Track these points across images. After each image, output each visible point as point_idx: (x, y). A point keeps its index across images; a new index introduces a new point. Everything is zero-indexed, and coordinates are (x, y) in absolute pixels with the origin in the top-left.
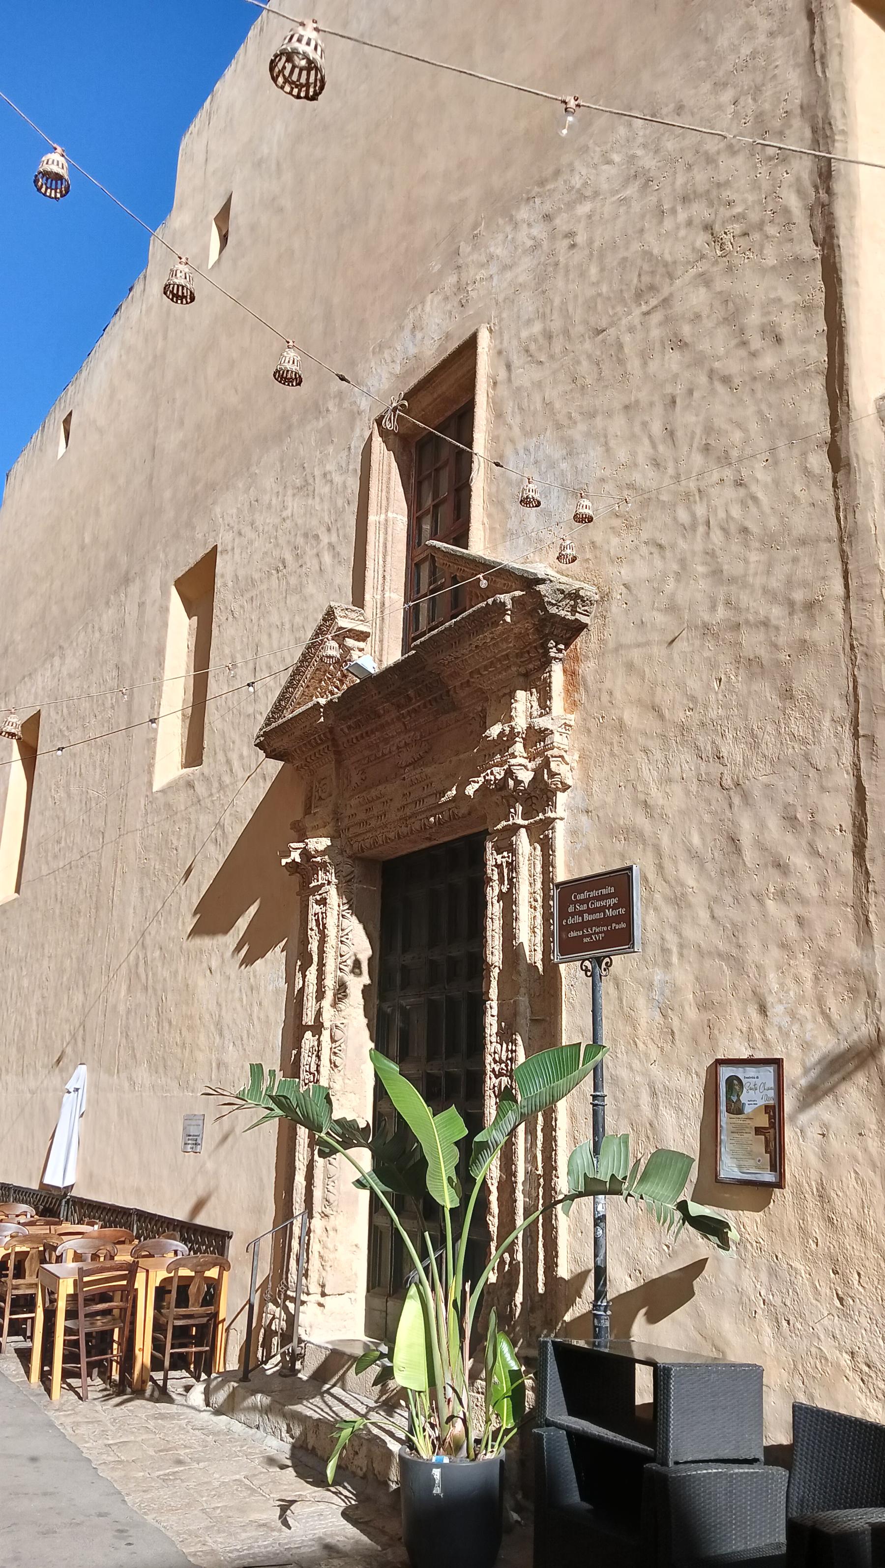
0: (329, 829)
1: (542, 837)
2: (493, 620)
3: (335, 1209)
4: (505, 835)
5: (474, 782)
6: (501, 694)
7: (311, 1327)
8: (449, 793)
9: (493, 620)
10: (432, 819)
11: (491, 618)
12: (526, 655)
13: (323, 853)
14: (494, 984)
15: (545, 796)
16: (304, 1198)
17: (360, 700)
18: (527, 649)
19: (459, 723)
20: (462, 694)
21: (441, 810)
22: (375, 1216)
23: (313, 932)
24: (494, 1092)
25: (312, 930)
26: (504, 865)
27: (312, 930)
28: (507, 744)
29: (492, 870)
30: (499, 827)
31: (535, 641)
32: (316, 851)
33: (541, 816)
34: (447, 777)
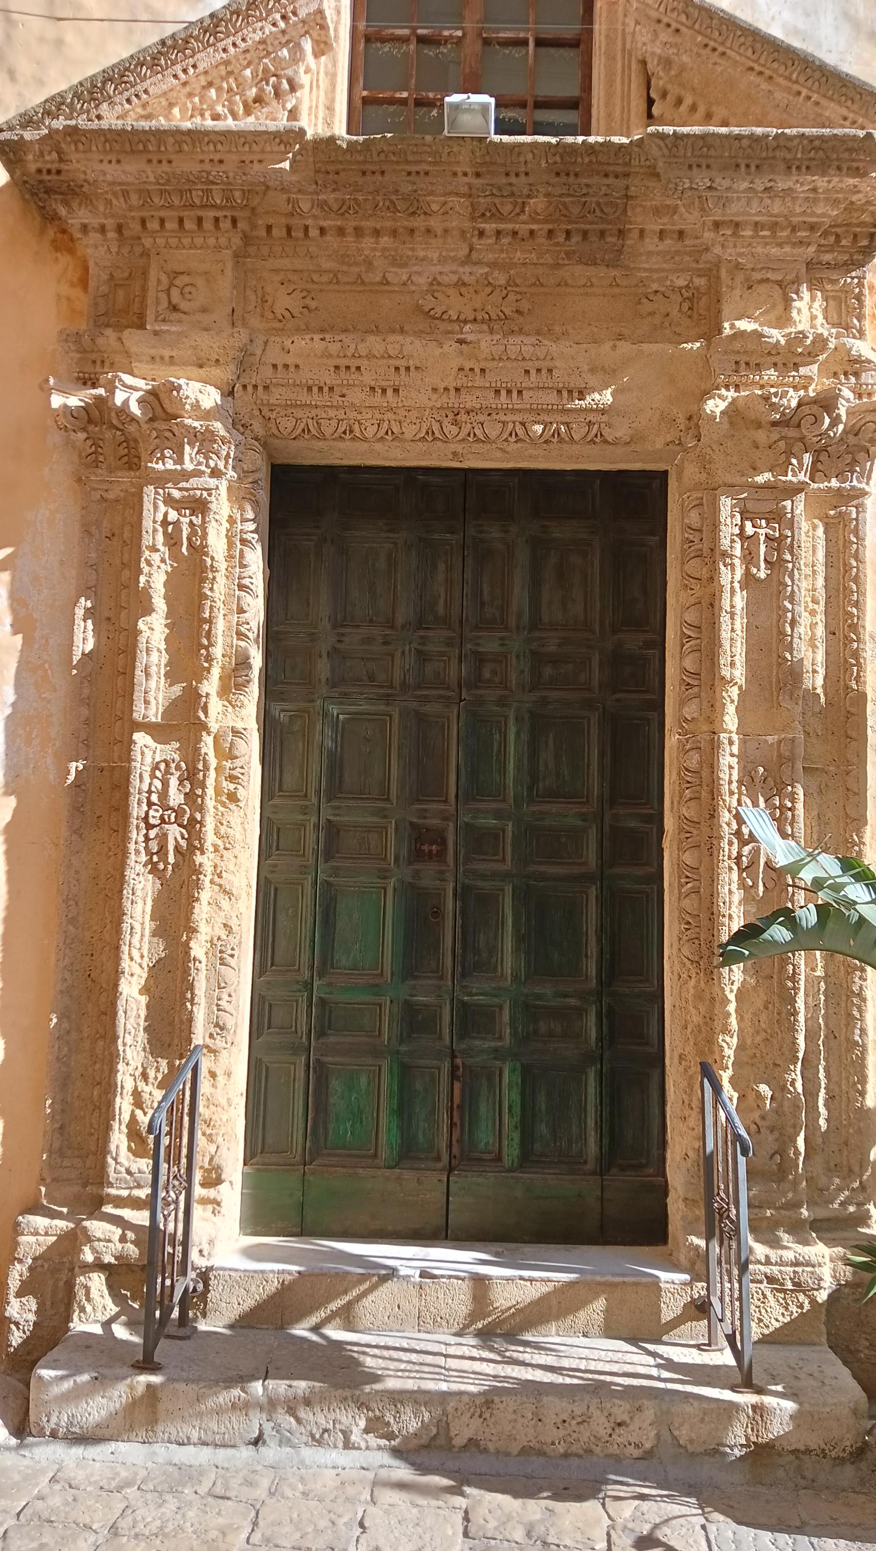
0: (226, 373)
1: (832, 512)
2: (855, 165)
3: (229, 1040)
4: (767, 494)
5: (720, 397)
6: (757, 276)
7: (211, 1242)
8: (596, 396)
9: (855, 165)
10: (538, 428)
11: (853, 160)
12: (832, 239)
13: (207, 415)
14: (731, 709)
15: (848, 458)
16: (142, 1023)
17: (414, 168)
18: (838, 230)
19: (617, 290)
20: (651, 244)
21: (565, 419)
22: (255, 1042)
23: (156, 557)
24: (738, 864)
25: (154, 549)
26: (762, 538)
27: (154, 549)
28: (798, 360)
29: (733, 541)
30: (760, 479)
31: (862, 224)
32: (196, 406)
33: (834, 483)
34: (593, 370)
